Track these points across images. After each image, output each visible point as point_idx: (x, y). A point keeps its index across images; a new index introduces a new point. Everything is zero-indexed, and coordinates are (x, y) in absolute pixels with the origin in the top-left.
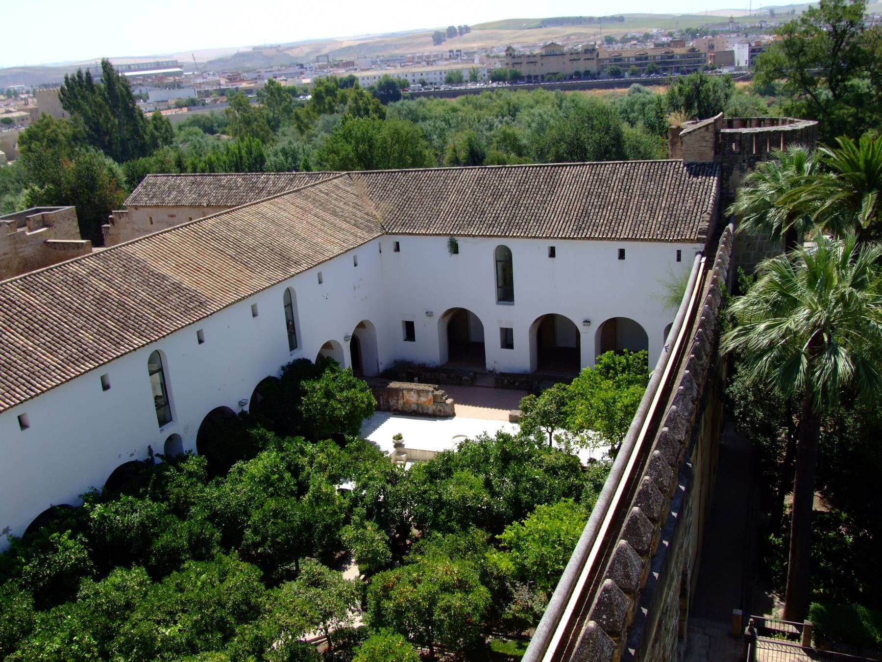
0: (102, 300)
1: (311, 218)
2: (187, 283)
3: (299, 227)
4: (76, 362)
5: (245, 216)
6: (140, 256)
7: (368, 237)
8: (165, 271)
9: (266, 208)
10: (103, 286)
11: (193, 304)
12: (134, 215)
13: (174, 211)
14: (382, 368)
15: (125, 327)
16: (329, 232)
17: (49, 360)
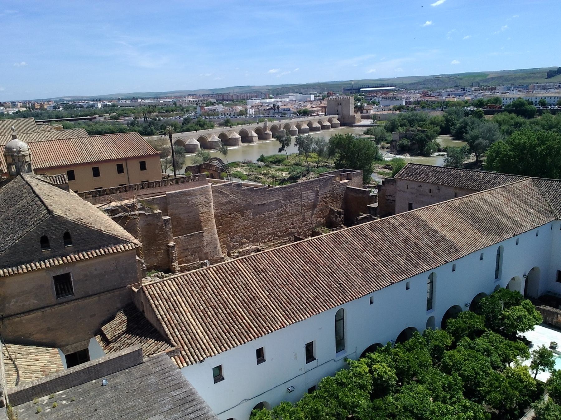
0: (406, 241)
1: (513, 205)
2: (448, 236)
3: (507, 210)
4: (397, 274)
5: (475, 197)
6: (424, 218)
7: (547, 220)
8: (437, 228)
9: (485, 195)
10: (407, 233)
11: (453, 249)
12: (398, 183)
13: (422, 184)
14: (539, 294)
15: (419, 258)
16: (523, 214)
17: (384, 270)
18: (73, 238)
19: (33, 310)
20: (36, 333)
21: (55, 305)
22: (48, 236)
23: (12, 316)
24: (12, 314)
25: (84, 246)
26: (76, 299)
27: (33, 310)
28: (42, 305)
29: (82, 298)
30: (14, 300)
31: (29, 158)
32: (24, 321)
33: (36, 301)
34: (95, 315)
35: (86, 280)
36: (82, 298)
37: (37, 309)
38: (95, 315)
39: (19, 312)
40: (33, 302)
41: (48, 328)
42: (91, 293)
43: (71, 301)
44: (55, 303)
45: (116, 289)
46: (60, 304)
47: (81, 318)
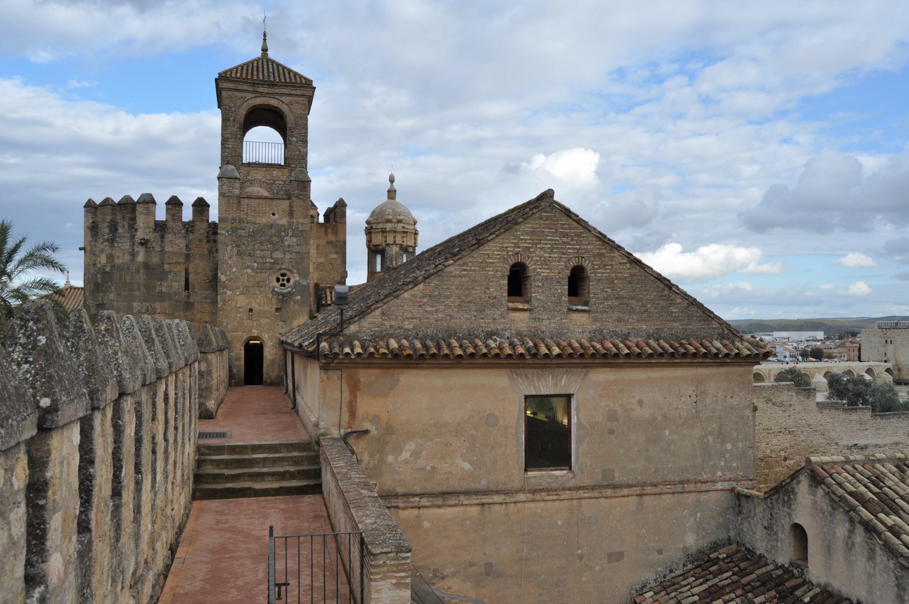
18: (594, 288)
19: (456, 493)
20: (455, 574)
21: (517, 492)
22: (531, 267)
23: (396, 496)
24: (400, 490)
25: (619, 320)
26: (578, 488)
27: (456, 493)
28: (483, 484)
29: (593, 488)
30: (411, 446)
31: (413, 241)
32: (426, 524)
33: (467, 466)
34: (620, 556)
35: (611, 432)
36: (593, 488)
37: (467, 493)
38: (620, 556)
39: (418, 490)
40: (459, 468)
41: (489, 565)
42: (618, 478)
43: (564, 489)
44: (517, 485)
45: (688, 482)
46: (534, 492)
47: (581, 557)
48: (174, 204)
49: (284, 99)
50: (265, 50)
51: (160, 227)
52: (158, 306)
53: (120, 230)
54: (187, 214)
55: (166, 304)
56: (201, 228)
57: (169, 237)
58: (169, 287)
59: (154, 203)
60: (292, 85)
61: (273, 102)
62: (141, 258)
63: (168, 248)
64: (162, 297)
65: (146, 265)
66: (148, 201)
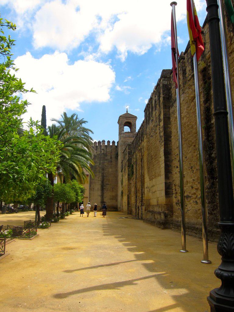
48: (109, 142)
49: (132, 120)
50: (127, 111)
51: (106, 146)
52: (105, 161)
53: (98, 147)
54: (111, 144)
55: (107, 161)
56: (114, 147)
57: (108, 148)
58: (108, 158)
59: (105, 141)
60: (133, 117)
61: (130, 121)
62: (102, 152)
63: (108, 150)
64: (106, 160)
65: (103, 153)
66: (104, 141)
